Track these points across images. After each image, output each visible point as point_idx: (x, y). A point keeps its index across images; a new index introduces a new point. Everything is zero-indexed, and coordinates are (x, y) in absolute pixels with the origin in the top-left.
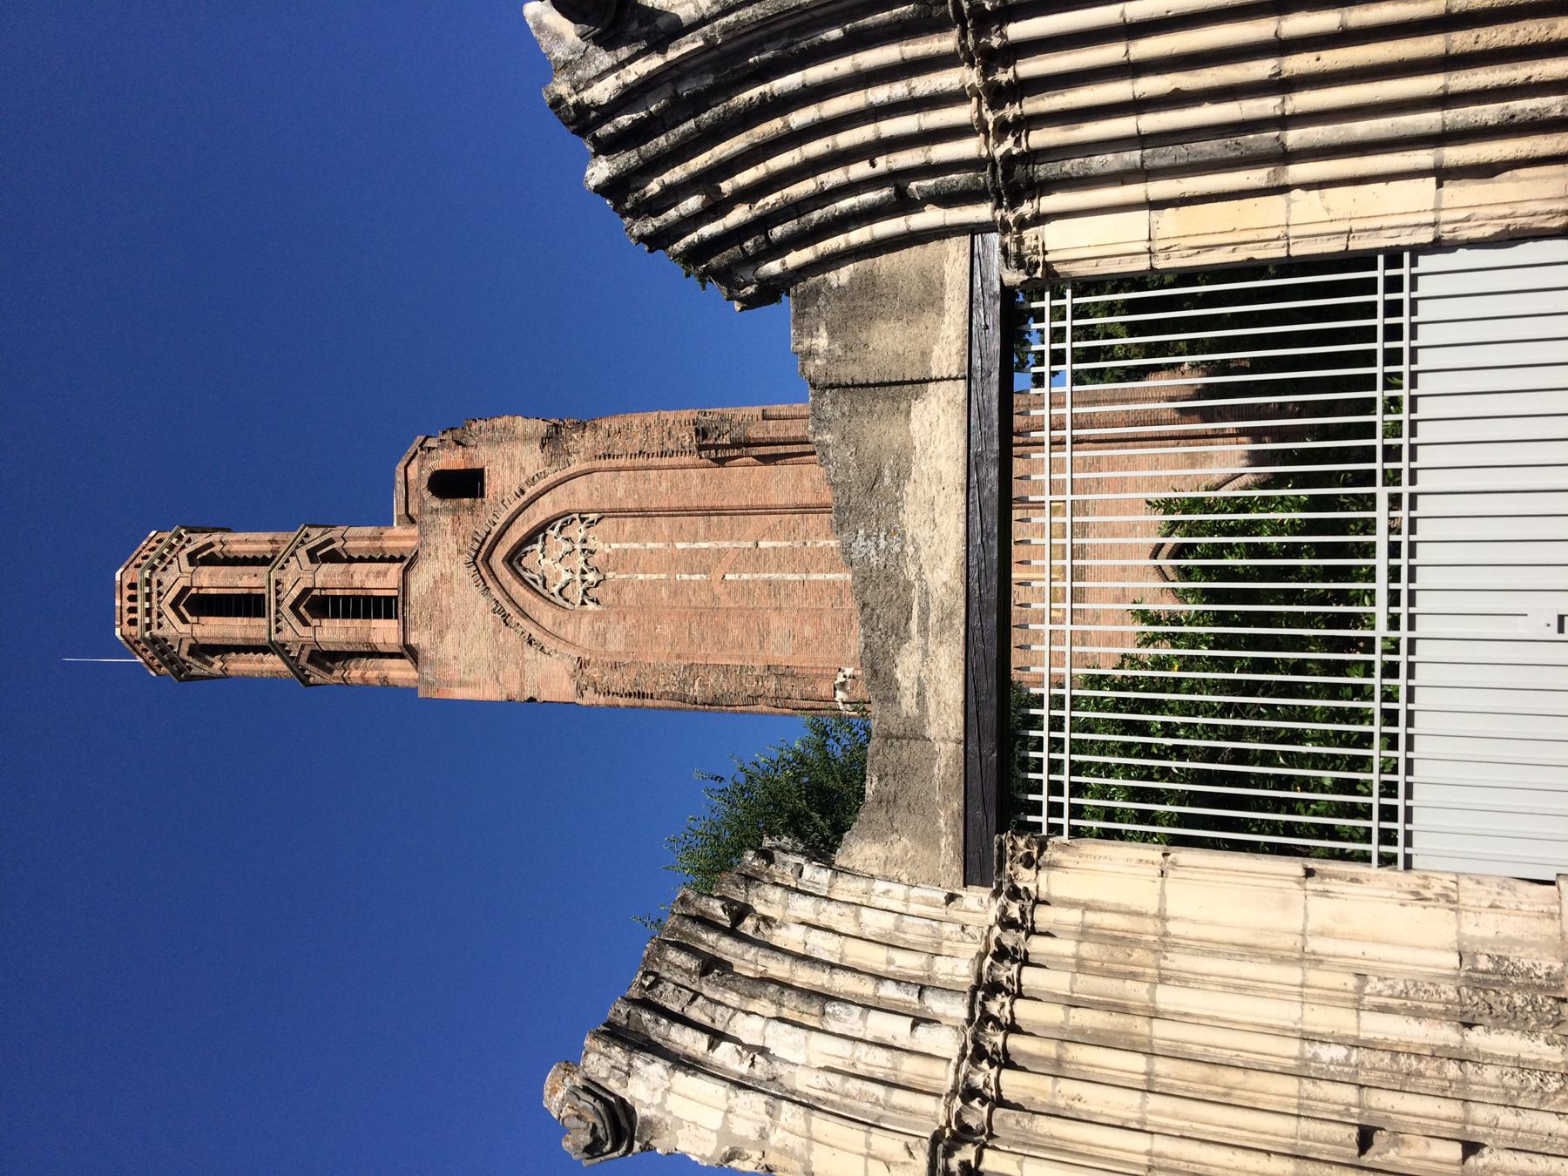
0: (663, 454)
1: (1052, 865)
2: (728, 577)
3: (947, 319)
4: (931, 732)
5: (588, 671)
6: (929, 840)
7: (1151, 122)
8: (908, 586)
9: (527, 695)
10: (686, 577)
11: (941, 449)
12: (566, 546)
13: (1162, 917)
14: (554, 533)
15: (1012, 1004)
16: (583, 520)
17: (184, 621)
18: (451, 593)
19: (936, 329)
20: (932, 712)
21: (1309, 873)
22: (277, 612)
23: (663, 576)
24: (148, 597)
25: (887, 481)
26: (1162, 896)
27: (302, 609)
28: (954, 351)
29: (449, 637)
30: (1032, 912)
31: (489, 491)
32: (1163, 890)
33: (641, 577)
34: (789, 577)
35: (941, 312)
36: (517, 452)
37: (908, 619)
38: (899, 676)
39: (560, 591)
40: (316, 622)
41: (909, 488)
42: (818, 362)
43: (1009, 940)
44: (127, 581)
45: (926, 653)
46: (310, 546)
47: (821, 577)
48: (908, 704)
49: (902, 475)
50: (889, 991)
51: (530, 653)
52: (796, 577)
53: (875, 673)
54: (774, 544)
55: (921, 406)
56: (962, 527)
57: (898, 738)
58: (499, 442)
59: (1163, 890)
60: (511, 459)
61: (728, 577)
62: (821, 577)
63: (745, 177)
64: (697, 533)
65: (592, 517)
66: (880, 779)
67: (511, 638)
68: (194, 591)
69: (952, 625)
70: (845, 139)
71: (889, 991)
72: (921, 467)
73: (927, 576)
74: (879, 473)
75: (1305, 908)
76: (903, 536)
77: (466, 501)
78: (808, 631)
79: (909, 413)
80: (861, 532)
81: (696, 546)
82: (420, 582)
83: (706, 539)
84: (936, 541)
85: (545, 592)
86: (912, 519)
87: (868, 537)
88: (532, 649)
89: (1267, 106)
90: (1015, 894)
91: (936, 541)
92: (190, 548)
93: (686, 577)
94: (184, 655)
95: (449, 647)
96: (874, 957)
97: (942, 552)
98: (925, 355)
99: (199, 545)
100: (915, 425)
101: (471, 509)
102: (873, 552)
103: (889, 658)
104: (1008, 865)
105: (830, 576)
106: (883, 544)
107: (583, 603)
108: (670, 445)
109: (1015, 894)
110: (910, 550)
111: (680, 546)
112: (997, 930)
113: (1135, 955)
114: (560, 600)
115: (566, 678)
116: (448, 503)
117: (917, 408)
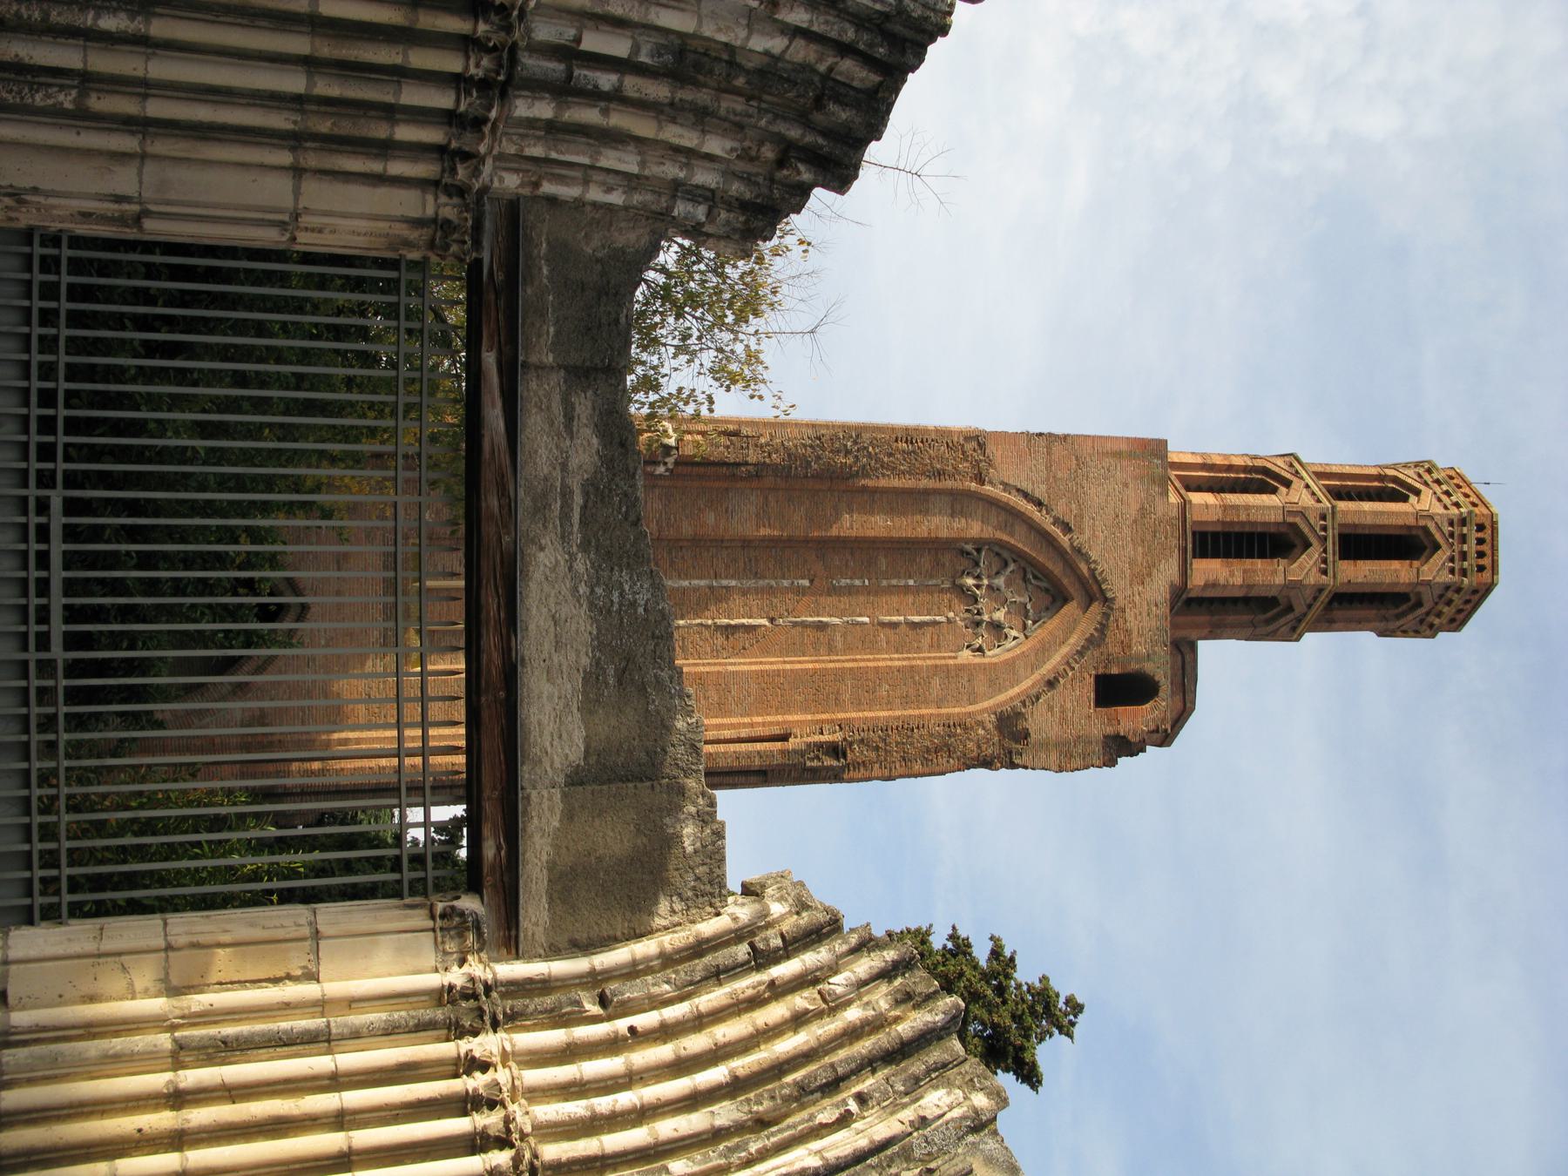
1: (418, 223)
2: (806, 583)
3: (544, 858)
4: (557, 378)
6: (562, 253)
7: (320, 1063)
8: (585, 546)
11: (548, 708)
13: (297, 171)
15: (467, 67)
17: (1425, 529)
18: (1132, 563)
19: (556, 847)
20: (556, 398)
21: (137, 220)
23: (885, 583)
24: (1464, 556)
25: (611, 671)
26: (297, 193)
27: (1297, 541)
28: (535, 820)
29: (1133, 510)
30: (443, 171)
32: (296, 199)
33: (911, 582)
35: (551, 866)
37: (584, 507)
38: (595, 441)
39: (1006, 564)
40: (1283, 529)
41: (585, 661)
42: (693, 809)
43: (465, 142)
44: (1487, 575)
45: (564, 466)
46: (1290, 616)
47: (695, 582)
48: (584, 406)
49: (592, 678)
50: (606, 81)
51: (1040, 492)
52: (725, 582)
53: (622, 445)
55: (571, 758)
56: (521, 614)
57: (596, 369)
59: (296, 199)
60: (1063, 720)
63: (776, 1012)
64: (844, 635)
66: (617, 321)
67: (1060, 509)
69: (534, 500)
70: (663, 1052)
71: (606, 81)
72: (571, 686)
73: (562, 559)
74: (620, 682)
75: (141, 182)
76: (592, 606)
77: (1115, 671)
78: (711, 518)
79: (587, 752)
80: (641, 610)
82: (1168, 571)
84: (552, 600)
85: (1023, 564)
86: (581, 624)
87: (633, 604)
89: (192, 1077)
90: (460, 191)
91: (552, 600)
92: (1423, 610)
95: (1134, 497)
96: (619, 120)
97: (546, 588)
98: (569, 815)
99: (1410, 617)
100: (579, 736)
101: (1109, 661)
102: (627, 587)
103: (607, 462)
104: (470, 223)
105: (686, 583)
106: (615, 596)
107: (979, 550)
109: (460, 191)
110: (583, 589)
112: (482, 149)
113: (329, 124)
114: (1005, 554)
115: (997, 461)
117: (575, 754)
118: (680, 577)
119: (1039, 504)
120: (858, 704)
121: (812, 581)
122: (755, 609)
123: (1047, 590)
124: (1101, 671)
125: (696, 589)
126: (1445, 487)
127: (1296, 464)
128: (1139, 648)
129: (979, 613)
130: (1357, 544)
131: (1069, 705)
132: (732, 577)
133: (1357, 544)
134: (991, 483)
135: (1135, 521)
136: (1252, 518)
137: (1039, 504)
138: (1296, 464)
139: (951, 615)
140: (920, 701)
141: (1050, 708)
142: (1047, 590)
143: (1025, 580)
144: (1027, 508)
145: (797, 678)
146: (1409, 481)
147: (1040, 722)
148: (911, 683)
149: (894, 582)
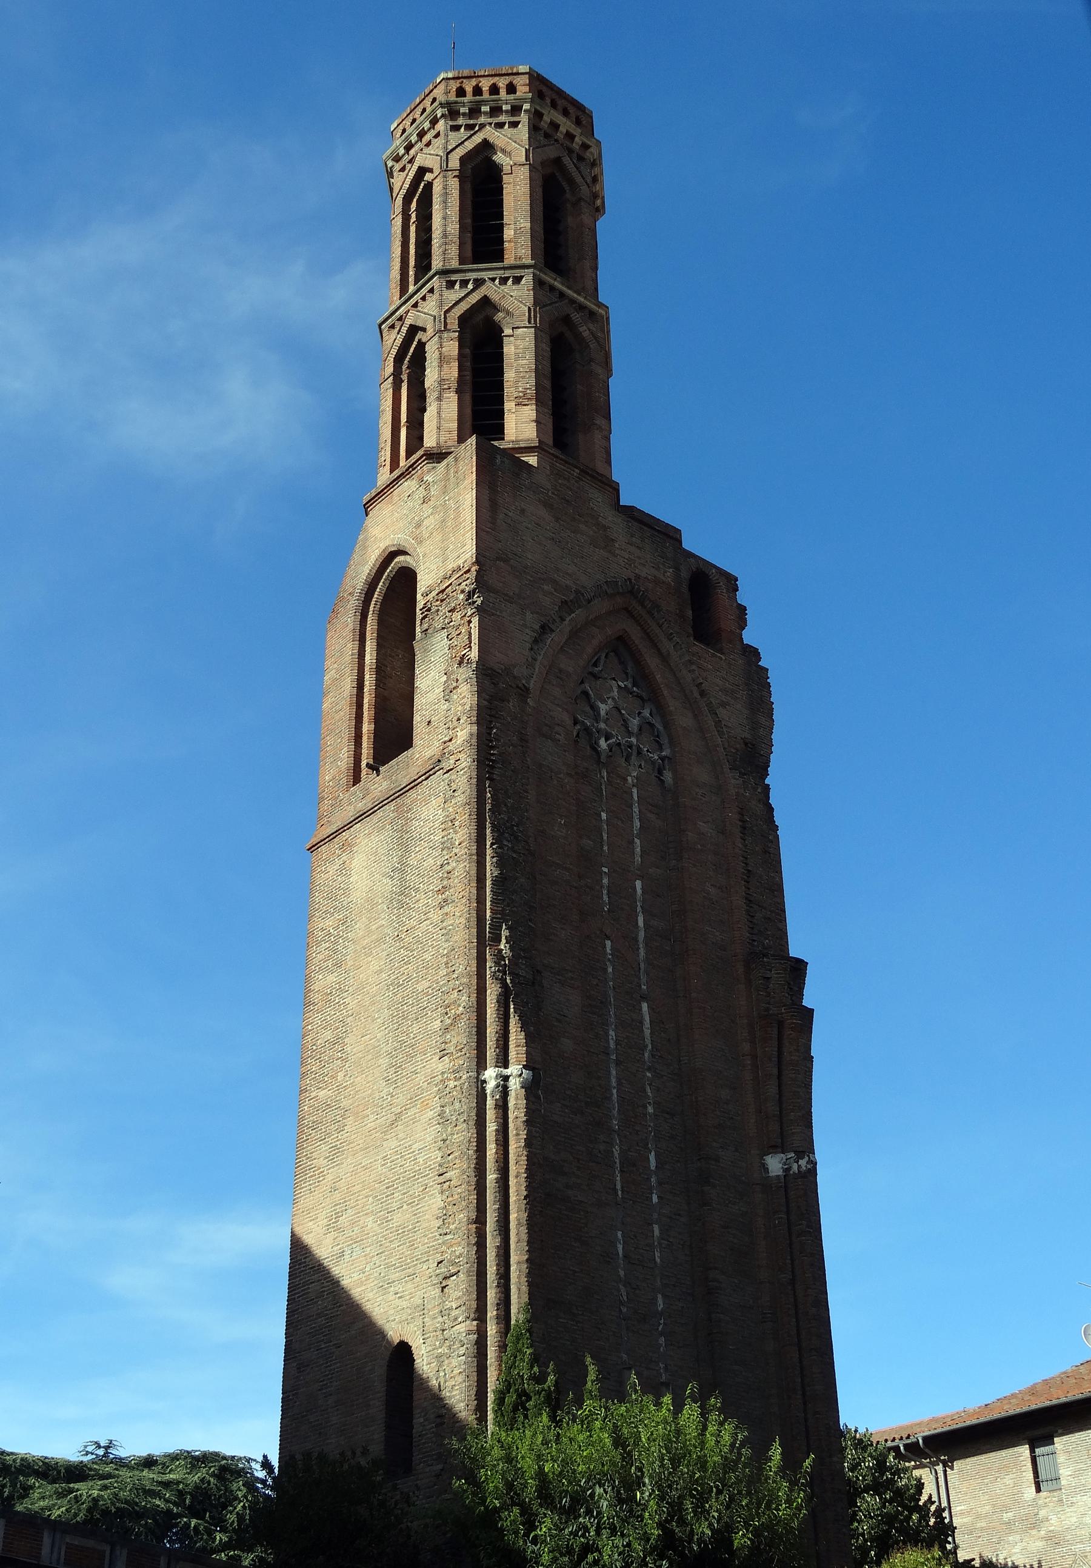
0: (749, 901)
10: (605, 881)
12: (634, 723)
14: (646, 713)
16: (663, 759)
22: (562, 295)
23: (605, 848)
31: (699, 647)
33: (604, 816)
39: (585, 694)
51: (532, 620)
52: (612, 1045)
61: (608, 943)
65: (668, 776)
68: (568, 196)
81: (639, 909)
88: (537, 627)
93: (605, 881)
105: (615, 1091)
107: (576, 722)
111: (638, 884)
116: (685, 589)
119: (545, 629)
121: (608, 938)
124: (691, 631)
125: (619, 1083)
126: (485, 109)
127: (453, 278)
130: (483, 238)
132: (607, 1035)
133: (483, 238)
135: (557, 519)
137: (545, 629)
138: (453, 278)
143: (596, 677)
146: (469, 145)
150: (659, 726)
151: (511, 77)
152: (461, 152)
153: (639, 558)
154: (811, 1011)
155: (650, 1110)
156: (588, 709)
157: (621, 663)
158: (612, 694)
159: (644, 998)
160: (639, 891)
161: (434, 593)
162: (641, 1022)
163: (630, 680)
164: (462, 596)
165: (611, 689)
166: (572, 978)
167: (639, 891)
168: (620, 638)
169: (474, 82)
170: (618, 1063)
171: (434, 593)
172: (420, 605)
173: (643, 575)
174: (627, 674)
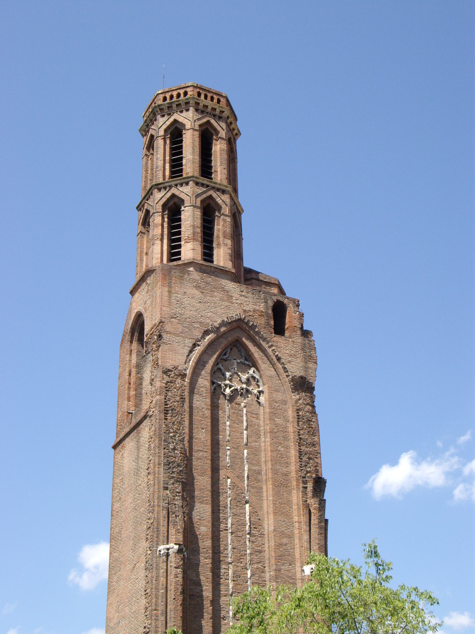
2: (229, 481)
5: (179, 380)
9: (164, 335)
10: (228, 453)
29: (197, 292)
31: (277, 338)
33: (228, 423)
34: (230, 521)
36: (299, 360)
39: (220, 369)
51: (189, 343)
52: (229, 525)
54: (248, 514)
58: (302, 349)
62: (229, 541)
77: (272, 322)
83: (249, 470)
93: (228, 453)
94: (176, 116)
105: (230, 547)
108: (304, 459)
111: (246, 451)
114: (215, 368)
116: (270, 311)
118: (227, 549)
119: (195, 345)
120: (287, 464)
121: (228, 478)
122: (241, 511)
123: (231, 349)
124: (273, 331)
125: (232, 541)
128: (262, 307)
129: (243, 389)
131: (288, 352)
134: (185, 370)
135: (203, 293)
136: (199, 225)
137: (195, 345)
139: (243, 404)
140: (285, 431)
141: (289, 362)
142: (231, 349)
143: (226, 360)
144: (198, 350)
145: (277, 494)
146: (168, 123)
147: (296, 369)
148: (277, 434)
149: (228, 432)
150: (257, 377)
151: (185, 89)
152: (165, 127)
153: (246, 301)
154: (325, 500)
155: (248, 551)
156: (221, 376)
157: (239, 351)
158: (233, 367)
159: (247, 502)
160: (246, 454)
161: (149, 335)
162: (245, 513)
163: (244, 358)
164: (156, 337)
165: (233, 365)
166: (207, 500)
167: (246, 454)
168: (237, 340)
169: (170, 94)
170: (232, 533)
171: (149, 335)
172: (145, 340)
173: (248, 309)
174: (241, 355)
